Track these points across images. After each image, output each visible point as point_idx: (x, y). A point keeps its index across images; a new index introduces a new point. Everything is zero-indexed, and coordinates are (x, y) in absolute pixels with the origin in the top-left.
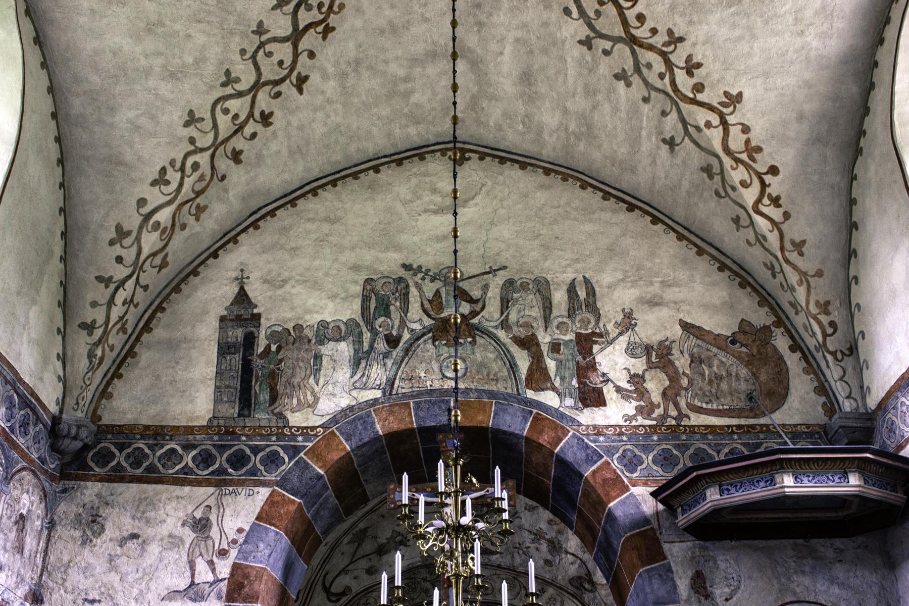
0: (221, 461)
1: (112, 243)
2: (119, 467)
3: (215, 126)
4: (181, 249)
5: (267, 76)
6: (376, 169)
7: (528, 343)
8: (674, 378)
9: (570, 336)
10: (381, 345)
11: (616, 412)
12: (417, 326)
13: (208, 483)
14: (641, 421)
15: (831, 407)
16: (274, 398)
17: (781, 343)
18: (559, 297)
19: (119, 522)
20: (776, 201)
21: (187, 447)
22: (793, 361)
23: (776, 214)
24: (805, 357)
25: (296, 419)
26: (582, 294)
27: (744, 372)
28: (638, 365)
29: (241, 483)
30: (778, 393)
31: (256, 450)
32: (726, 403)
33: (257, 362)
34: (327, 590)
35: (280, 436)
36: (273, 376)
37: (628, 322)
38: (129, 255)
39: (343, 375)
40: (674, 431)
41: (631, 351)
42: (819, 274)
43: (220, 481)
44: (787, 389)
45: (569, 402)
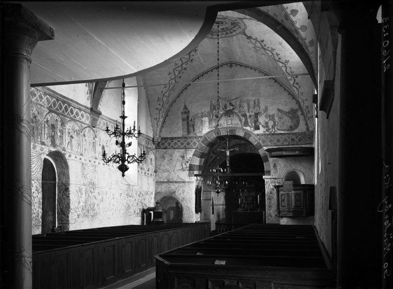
0: (185, 144)
1: (158, 101)
2: (166, 146)
3: (175, 74)
4: (171, 99)
5: (184, 62)
6: (212, 71)
7: (245, 115)
8: (275, 123)
9: (254, 114)
10: (214, 117)
11: (262, 130)
12: (221, 113)
13: (183, 149)
14: (267, 133)
15: (308, 129)
16: (194, 130)
17: (299, 113)
18: (252, 103)
19: (167, 158)
20: (297, 84)
21: (179, 141)
22: (301, 118)
23: (298, 87)
24: (304, 116)
25: (198, 135)
26: (257, 103)
27: (290, 120)
28: (267, 120)
29: (190, 148)
30: (297, 125)
31: (191, 141)
32: (285, 128)
33: (190, 123)
34: (213, 152)
35: (196, 138)
36: (193, 126)
37: (266, 109)
38: (161, 103)
39: (207, 124)
40: (273, 134)
41: (266, 117)
42: (306, 100)
43: (185, 148)
44: (299, 124)
45: (252, 129)
